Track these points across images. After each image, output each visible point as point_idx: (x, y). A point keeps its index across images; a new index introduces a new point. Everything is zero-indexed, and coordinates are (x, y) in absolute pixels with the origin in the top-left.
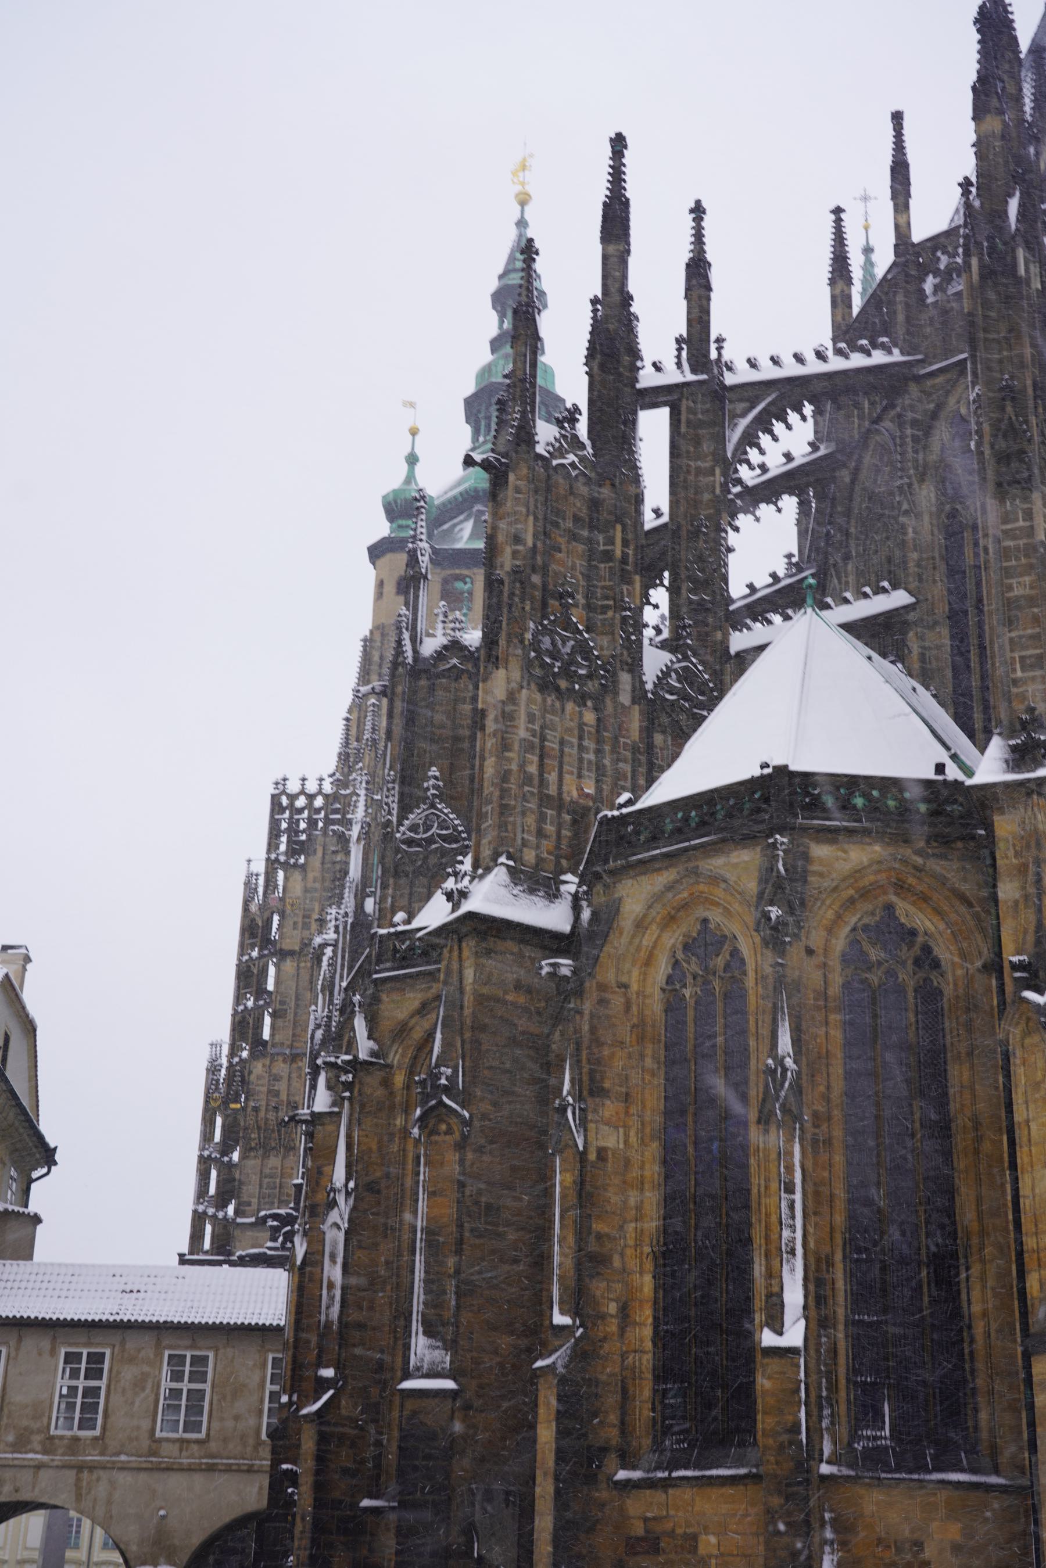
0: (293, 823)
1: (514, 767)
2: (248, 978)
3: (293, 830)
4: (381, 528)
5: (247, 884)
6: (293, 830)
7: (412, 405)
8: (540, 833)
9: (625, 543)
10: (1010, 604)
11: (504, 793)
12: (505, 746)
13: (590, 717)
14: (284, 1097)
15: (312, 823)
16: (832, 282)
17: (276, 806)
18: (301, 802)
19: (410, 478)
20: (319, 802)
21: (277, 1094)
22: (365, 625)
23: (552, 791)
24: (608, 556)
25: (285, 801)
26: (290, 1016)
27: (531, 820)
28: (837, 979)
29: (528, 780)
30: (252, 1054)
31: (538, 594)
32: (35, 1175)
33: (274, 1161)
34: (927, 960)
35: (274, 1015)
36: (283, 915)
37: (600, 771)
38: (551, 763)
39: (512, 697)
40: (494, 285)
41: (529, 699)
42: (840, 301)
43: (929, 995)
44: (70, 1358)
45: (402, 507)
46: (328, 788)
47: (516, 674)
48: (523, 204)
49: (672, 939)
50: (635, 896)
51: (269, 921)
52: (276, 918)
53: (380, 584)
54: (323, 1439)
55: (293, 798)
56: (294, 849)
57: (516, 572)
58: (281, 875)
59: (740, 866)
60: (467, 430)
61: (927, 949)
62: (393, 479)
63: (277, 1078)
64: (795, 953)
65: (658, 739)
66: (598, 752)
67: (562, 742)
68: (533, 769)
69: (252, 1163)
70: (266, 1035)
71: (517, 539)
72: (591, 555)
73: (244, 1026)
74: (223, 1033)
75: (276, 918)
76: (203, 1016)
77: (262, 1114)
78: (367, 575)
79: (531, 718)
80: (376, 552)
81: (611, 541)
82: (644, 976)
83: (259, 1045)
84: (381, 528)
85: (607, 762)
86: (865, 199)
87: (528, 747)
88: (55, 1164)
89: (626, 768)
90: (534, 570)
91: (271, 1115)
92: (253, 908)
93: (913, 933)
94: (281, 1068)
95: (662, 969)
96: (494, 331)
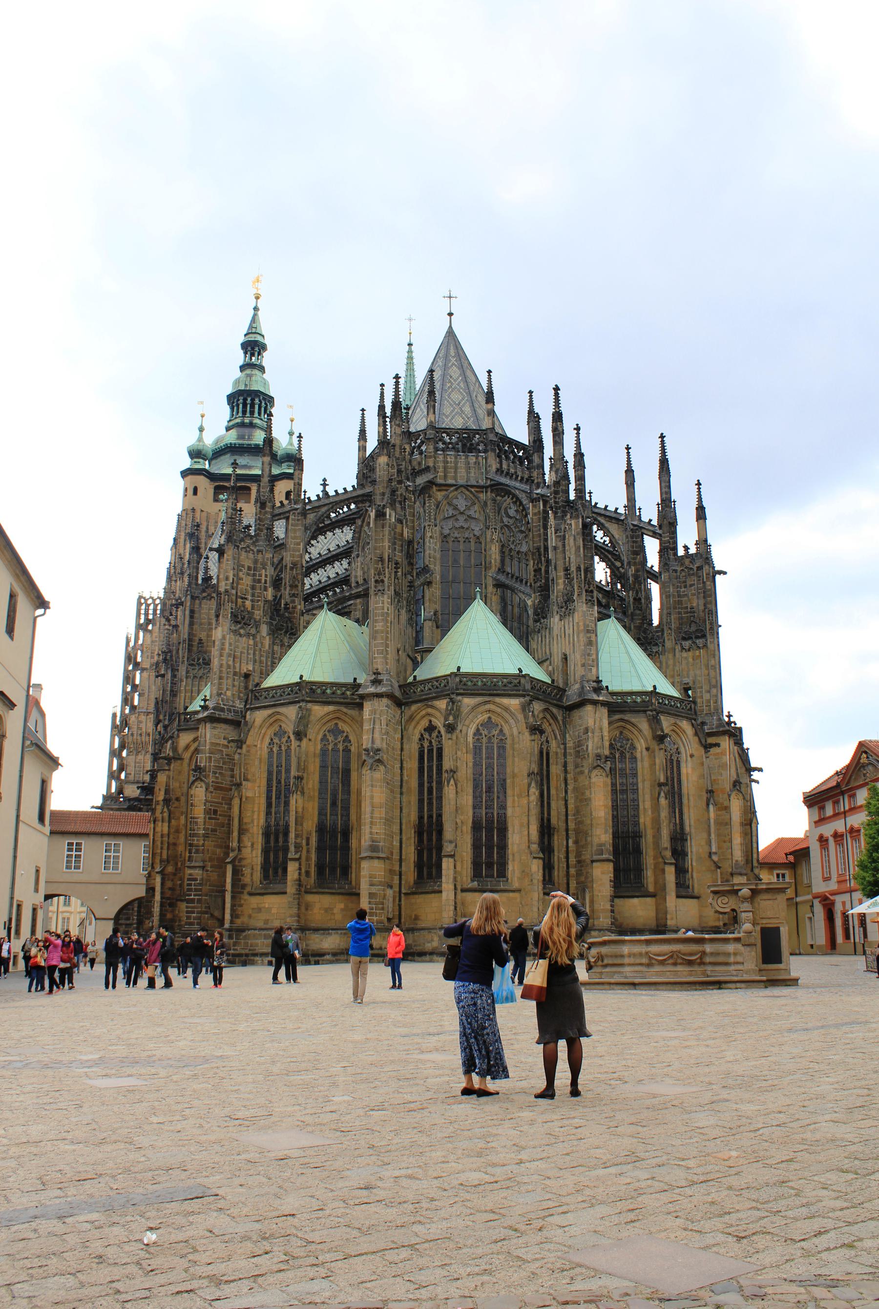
0: (147, 610)
1: (224, 662)
2: (128, 679)
3: (147, 614)
4: (187, 463)
5: (127, 638)
6: (147, 614)
7: (202, 403)
8: (234, 686)
9: (266, 576)
10: (377, 632)
11: (221, 672)
12: (221, 655)
13: (251, 642)
14: (144, 730)
15: (155, 610)
16: (359, 440)
17: (139, 604)
18: (150, 601)
19: (200, 439)
20: (158, 601)
21: (141, 729)
22: (179, 511)
23: (238, 670)
24: (259, 581)
25: (143, 601)
26: (146, 696)
27: (230, 681)
28: (319, 747)
29: (229, 666)
30: (130, 711)
31: (234, 598)
33: (140, 757)
34: (347, 739)
35: (139, 695)
36: (142, 651)
37: (255, 661)
38: (237, 660)
39: (224, 637)
40: (242, 339)
41: (230, 637)
42: (362, 448)
43: (347, 751)
44: (69, 844)
45: (195, 454)
46: (162, 595)
47: (226, 628)
48: (257, 298)
49: (270, 732)
50: (258, 717)
51: (136, 654)
52: (139, 653)
53: (186, 490)
55: (146, 600)
56: (148, 621)
57: (226, 591)
58: (141, 634)
59: (291, 712)
60: (228, 409)
61: (347, 736)
62: (191, 440)
63: (141, 722)
64: (305, 740)
65: (276, 648)
66: (254, 654)
67: (241, 653)
68: (231, 663)
69: (132, 757)
70: (136, 703)
71: (227, 579)
72: (254, 581)
73: (126, 699)
74: (118, 700)
75: (139, 653)
76: (109, 698)
77: (135, 737)
78: (180, 484)
79: (230, 644)
80: (185, 474)
81: (260, 575)
82: (261, 743)
83: (133, 708)
84: (187, 463)
85: (257, 658)
86: (410, 320)
87: (229, 655)
89: (264, 659)
90: (233, 588)
91: (139, 738)
92: (130, 649)
93: (343, 732)
94: (143, 718)
95: (267, 740)
96: (241, 363)
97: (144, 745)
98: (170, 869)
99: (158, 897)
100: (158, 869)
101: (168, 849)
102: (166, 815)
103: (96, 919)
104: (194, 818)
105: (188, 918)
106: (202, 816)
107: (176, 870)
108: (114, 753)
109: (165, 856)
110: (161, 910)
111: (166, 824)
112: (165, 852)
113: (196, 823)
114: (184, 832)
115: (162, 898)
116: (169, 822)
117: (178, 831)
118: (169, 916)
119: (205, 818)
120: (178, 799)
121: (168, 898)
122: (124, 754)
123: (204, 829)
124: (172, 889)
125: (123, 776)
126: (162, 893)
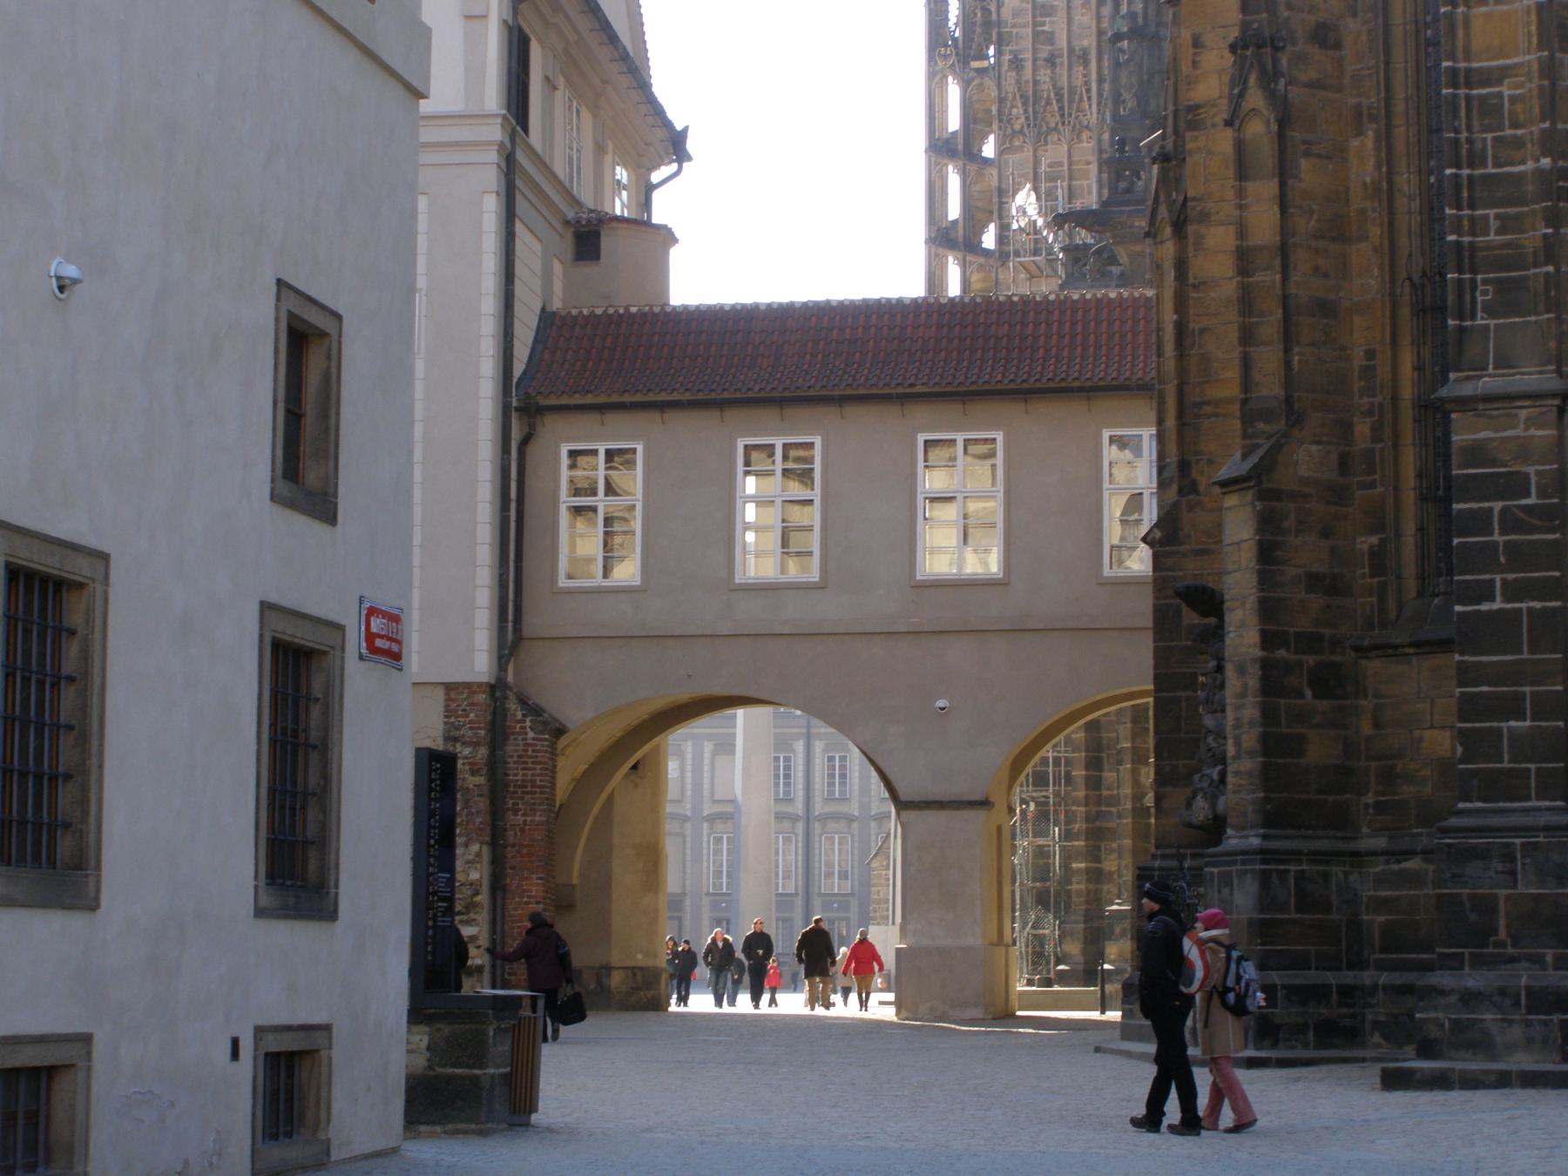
14: (1062, 42)
21: (1050, 38)
32: (656, 177)
54: (1268, 524)
77: (1028, 73)
88: (689, 158)
91: (1044, 75)
97: (1067, 101)
98: (1307, 461)
99: (1242, 635)
100: (1233, 465)
101: (1288, 338)
102: (1258, 129)
103: (902, 805)
104: (1471, 78)
105: (1477, 745)
106: (1528, 58)
107: (1344, 464)
108: (941, 148)
109: (1270, 387)
110: (1269, 715)
111: (1264, 190)
112: (1268, 359)
113: (1490, 110)
114: (1375, 232)
115: (1269, 640)
116: (1284, 172)
117: (1337, 231)
118: (1319, 751)
119: (1549, 69)
120: (1325, 36)
121: (1309, 642)
122: (989, 150)
123: (1548, 143)
124: (1330, 585)
125: (989, 240)
126: (1268, 609)
